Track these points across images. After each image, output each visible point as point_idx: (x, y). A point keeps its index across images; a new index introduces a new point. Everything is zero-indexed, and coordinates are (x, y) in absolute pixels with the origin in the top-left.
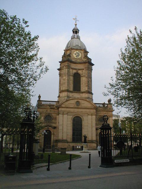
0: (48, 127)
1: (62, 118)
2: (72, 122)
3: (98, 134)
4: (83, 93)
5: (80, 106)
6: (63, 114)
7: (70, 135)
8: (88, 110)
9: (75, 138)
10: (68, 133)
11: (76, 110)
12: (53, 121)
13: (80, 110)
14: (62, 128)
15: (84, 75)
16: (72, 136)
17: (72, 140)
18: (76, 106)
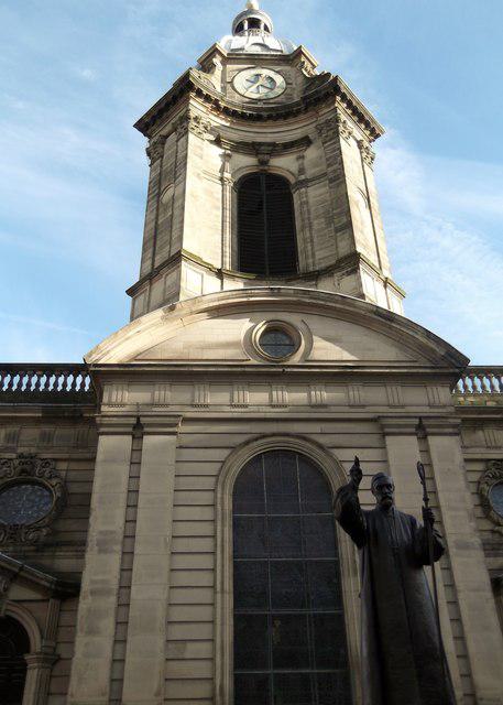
4: (315, 276)
5: (296, 359)
6: (137, 428)
8: (376, 397)
9: (262, 683)
10: (178, 632)
11: (256, 399)
13: (294, 397)
15: (310, 173)
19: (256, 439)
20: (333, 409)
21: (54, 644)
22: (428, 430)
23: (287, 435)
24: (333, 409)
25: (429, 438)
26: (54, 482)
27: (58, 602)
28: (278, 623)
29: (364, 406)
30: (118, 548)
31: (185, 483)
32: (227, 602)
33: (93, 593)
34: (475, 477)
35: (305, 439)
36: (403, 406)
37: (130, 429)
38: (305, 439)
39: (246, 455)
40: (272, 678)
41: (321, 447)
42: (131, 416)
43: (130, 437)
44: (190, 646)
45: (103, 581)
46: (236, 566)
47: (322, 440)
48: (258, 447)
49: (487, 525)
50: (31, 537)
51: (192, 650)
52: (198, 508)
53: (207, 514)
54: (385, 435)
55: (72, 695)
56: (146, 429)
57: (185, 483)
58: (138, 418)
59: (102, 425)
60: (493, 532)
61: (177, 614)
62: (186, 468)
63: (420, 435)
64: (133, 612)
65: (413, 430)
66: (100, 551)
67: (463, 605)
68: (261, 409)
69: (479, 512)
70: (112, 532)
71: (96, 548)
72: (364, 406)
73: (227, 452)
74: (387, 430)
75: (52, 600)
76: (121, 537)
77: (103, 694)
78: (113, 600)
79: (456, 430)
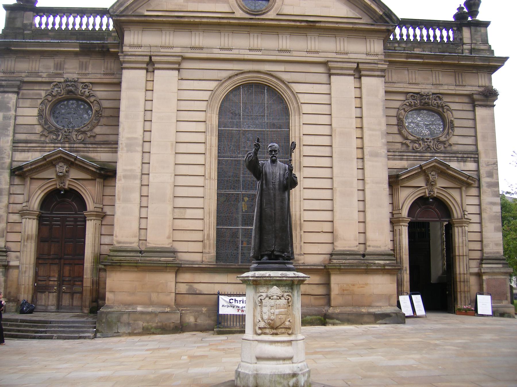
0: (61, 168)
1: (141, 95)
2: (215, 120)
3: (405, 212)
7: (199, 213)
9: (234, 234)
10: (180, 202)
12: (98, 130)
14: (137, 168)
16: (213, 220)
17: (213, 252)
18: (240, 13)
19: (237, 75)
20: (295, 53)
21: (101, 206)
22: (363, 73)
23: (258, 72)
24: (295, 53)
25: (363, 78)
26: (92, 99)
27: (102, 180)
28: (246, 199)
29: (318, 52)
30: (140, 149)
31: (184, 105)
32: (213, 185)
33: (125, 177)
34: (397, 104)
35: (272, 76)
36: (347, 53)
37: (144, 66)
38: (272, 76)
39: (229, 86)
40: (241, 231)
41: (283, 82)
42: (146, 56)
43: (145, 71)
44: (188, 211)
45: (131, 170)
46: (219, 163)
47: (285, 77)
48: (238, 80)
49: (399, 139)
50: (80, 137)
51: (189, 213)
52: (195, 123)
53: (201, 127)
54: (330, 75)
55: (116, 236)
56: (156, 66)
57: (184, 105)
58: (150, 57)
59: (124, 62)
60: (402, 144)
61: (180, 192)
62: (186, 95)
63: (357, 76)
64: (152, 190)
65: (352, 72)
66: (128, 151)
67: (367, 191)
68: (242, 52)
69: (395, 129)
70: (136, 139)
71: (125, 149)
72: (318, 52)
73: (215, 84)
74: (333, 71)
75: (98, 180)
76: (141, 142)
77: (135, 237)
78: (138, 182)
79: (383, 74)
